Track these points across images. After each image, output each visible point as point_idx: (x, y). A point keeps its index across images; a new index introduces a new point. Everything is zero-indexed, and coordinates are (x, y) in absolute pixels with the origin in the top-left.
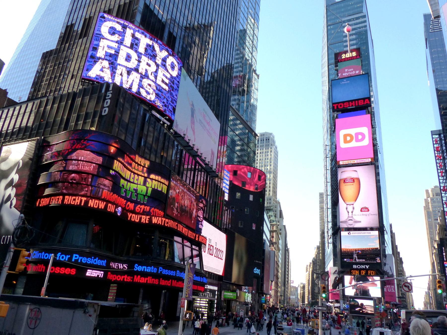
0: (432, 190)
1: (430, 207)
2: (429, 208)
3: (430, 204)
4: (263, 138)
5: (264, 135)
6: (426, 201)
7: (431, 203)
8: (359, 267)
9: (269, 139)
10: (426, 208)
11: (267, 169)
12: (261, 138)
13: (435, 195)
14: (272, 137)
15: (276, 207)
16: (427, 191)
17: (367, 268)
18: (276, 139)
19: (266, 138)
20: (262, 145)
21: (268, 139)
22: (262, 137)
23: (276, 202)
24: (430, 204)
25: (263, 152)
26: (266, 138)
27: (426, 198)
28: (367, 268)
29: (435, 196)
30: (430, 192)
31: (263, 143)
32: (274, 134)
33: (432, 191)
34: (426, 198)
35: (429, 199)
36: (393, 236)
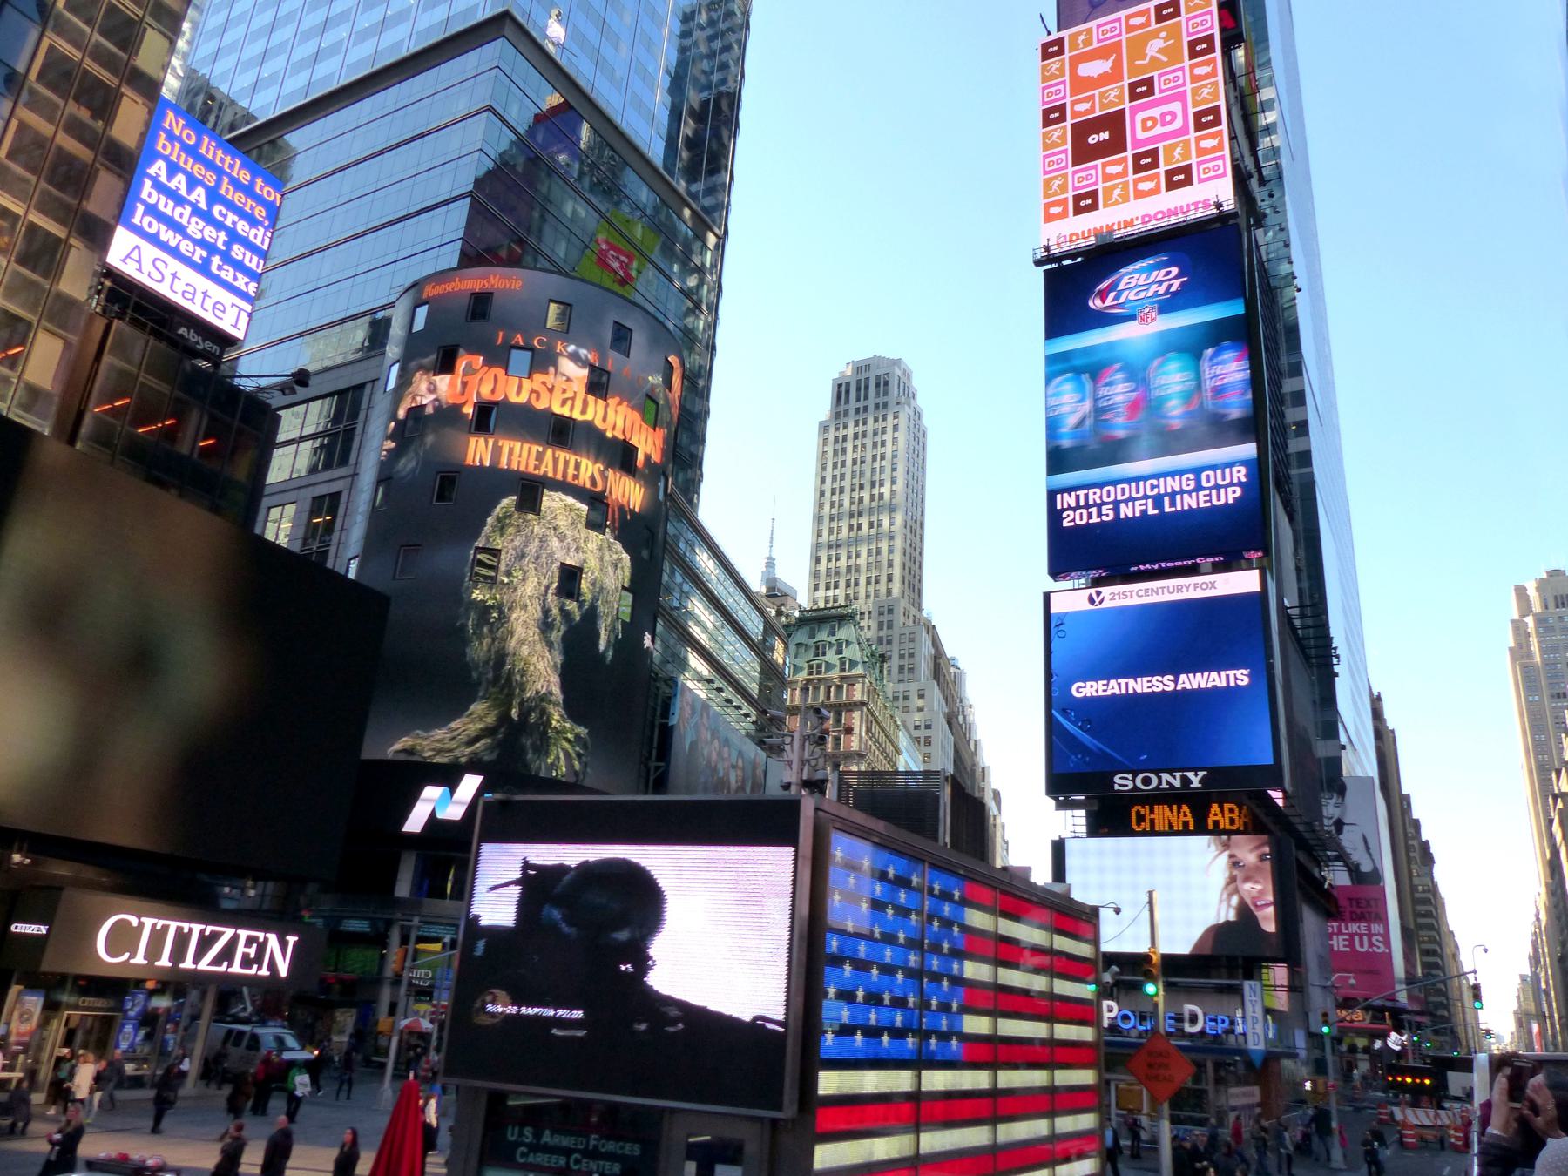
0: (1542, 585)
1: (1535, 648)
2: (1529, 655)
3: (1534, 640)
4: (867, 379)
5: (868, 367)
6: (1518, 627)
7: (1538, 634)
8: (1147, 781)
9: (886, 383)
10: (1520, 653)
11: (881, 496)
12: (859, 381)
13: (1551, 604)
14: (898, 372)
15: (912, 640)
16: (1521, 592)
17: (1196, 783)
18: (917, 383)
19: (878, 377)
20: (861, 405)
21: (883, 384)
22: (863, 376)
23: (917, 621)
24: (1534, 640)
25: (864, 435)
26: (878, 377)
27: (1516, 616)
28: (1196, 783)
29: (1552, 609)
30: (1532, 593)
31: (866, 398)
32: (910, 362)
33: (1538, 589)
34: (1516, 616)
35: (1530, 620)
36: (1384, 740)
